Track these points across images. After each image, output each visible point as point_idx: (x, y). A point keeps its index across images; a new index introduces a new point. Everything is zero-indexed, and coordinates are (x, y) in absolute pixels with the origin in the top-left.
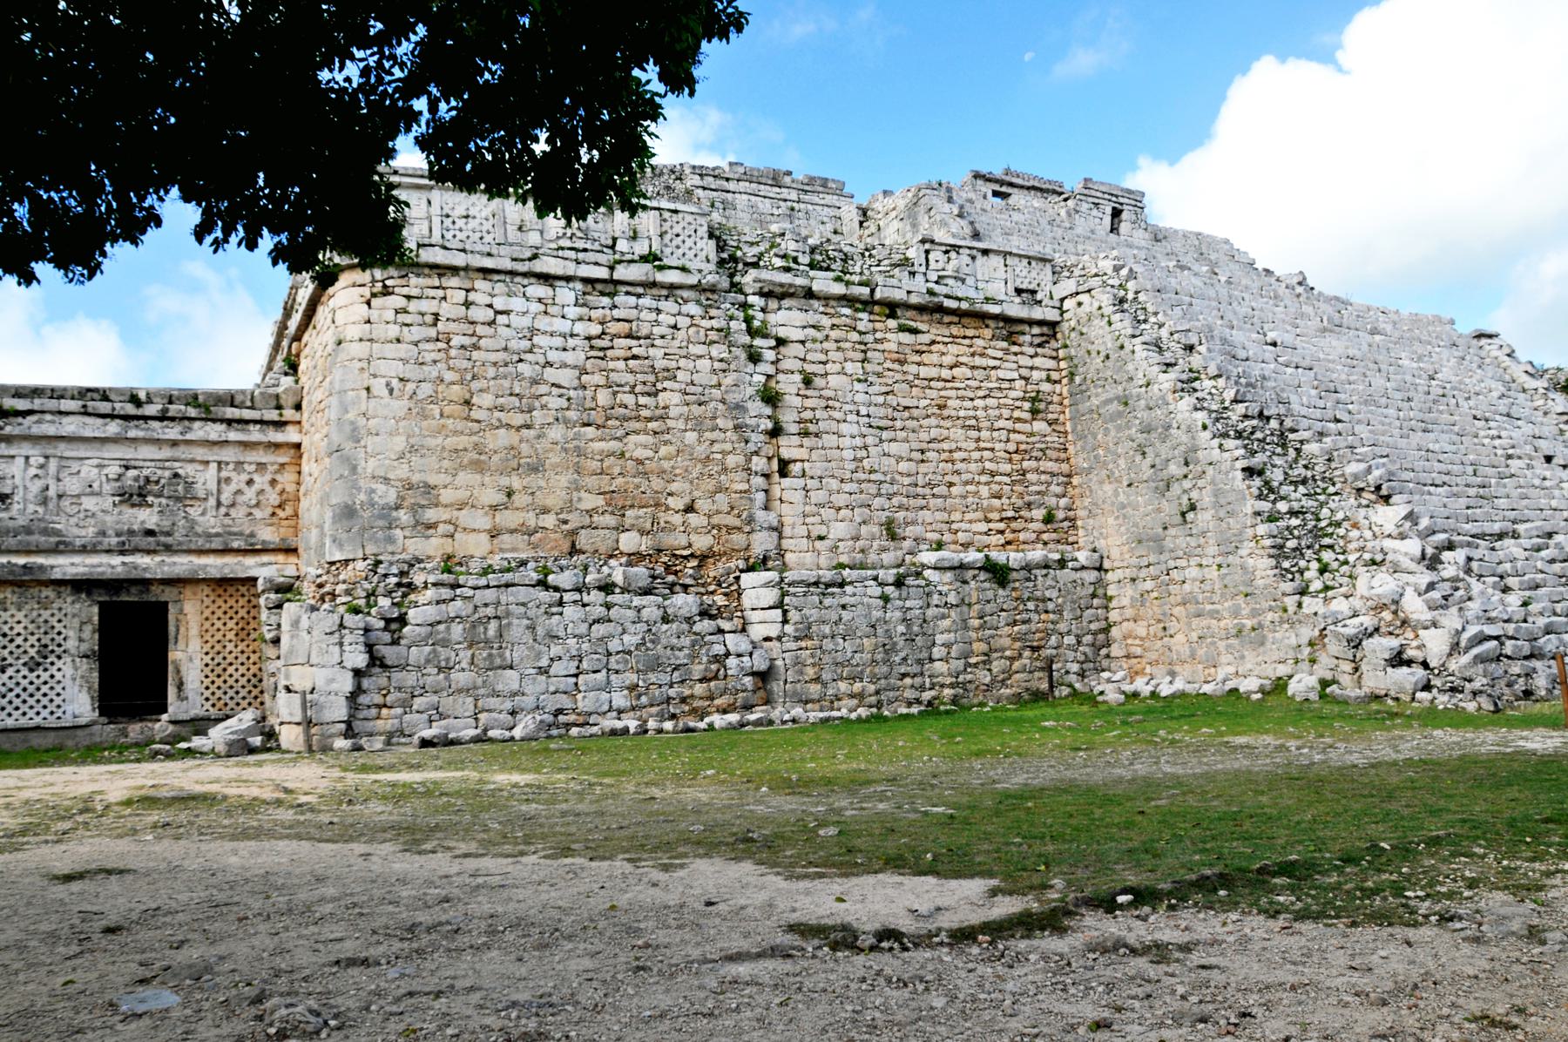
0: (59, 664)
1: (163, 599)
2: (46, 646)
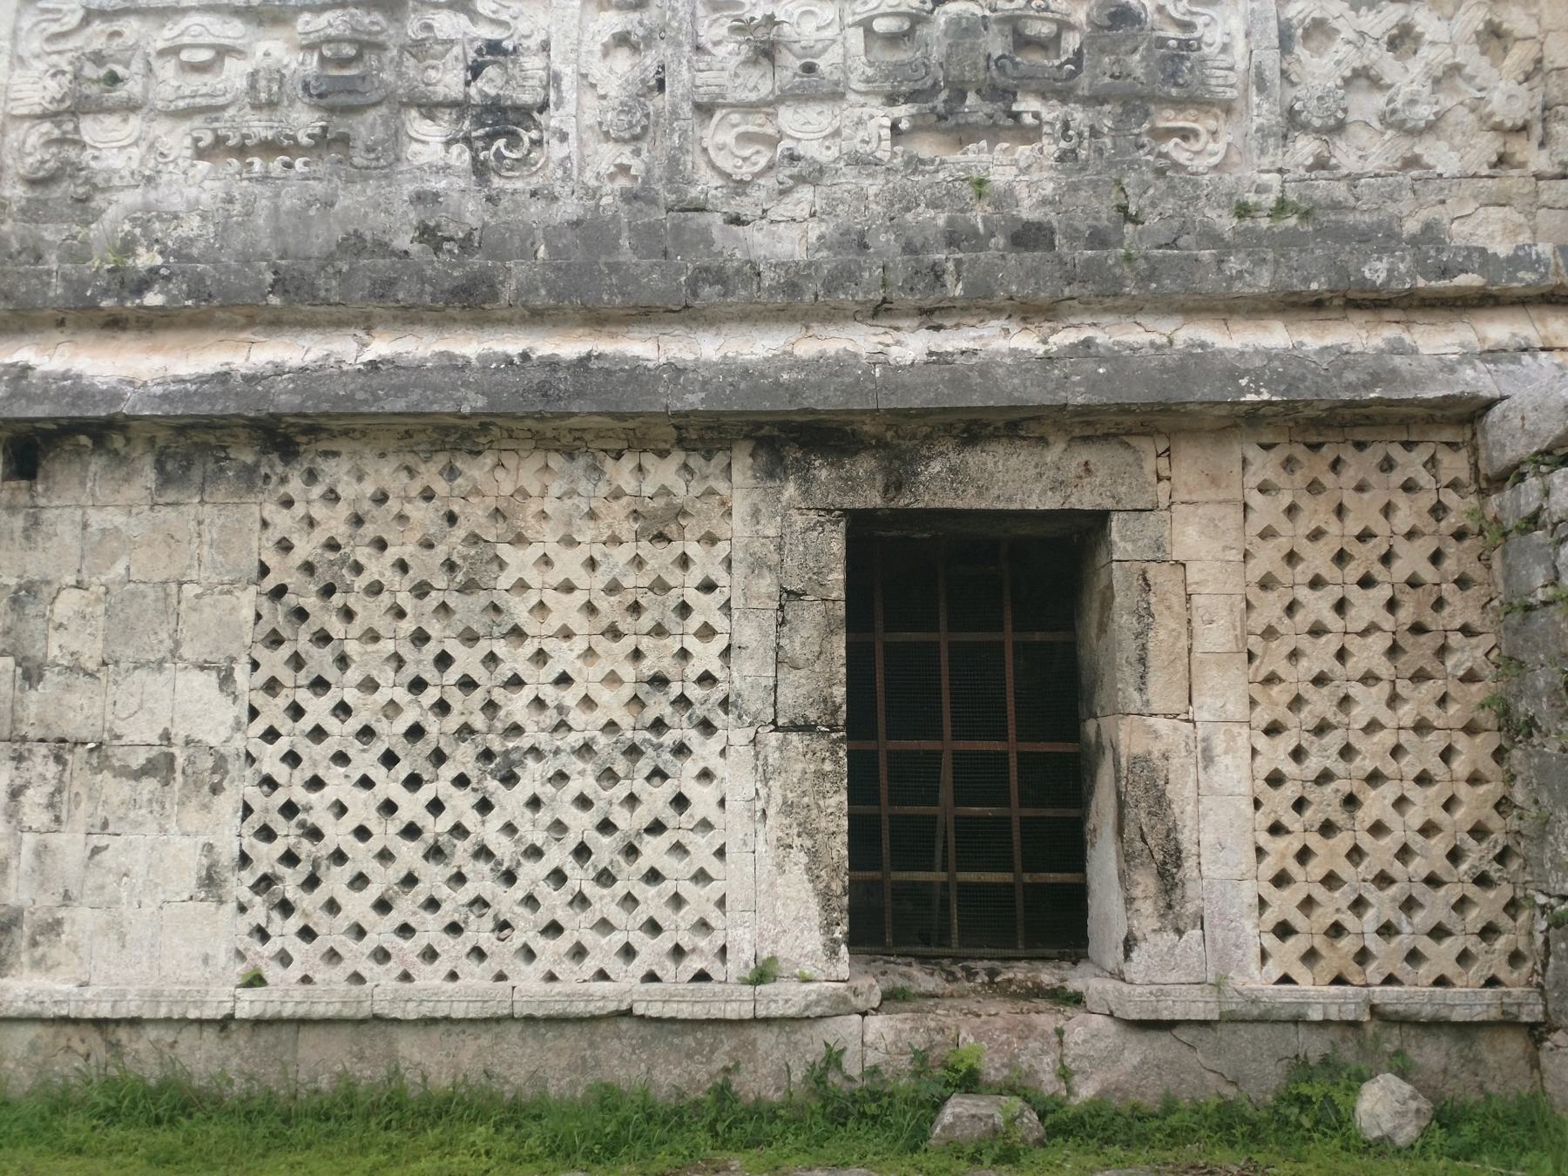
0: (705, 751)
1: (1085, 499)
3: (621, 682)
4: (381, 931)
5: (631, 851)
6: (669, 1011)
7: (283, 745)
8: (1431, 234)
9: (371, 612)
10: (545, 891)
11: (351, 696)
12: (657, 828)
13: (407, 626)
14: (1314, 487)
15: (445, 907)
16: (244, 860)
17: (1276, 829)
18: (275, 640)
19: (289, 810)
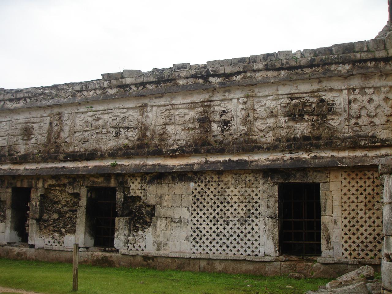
0: (256, 221)
2: (249, 210)
3: (243, 210)
4: (210, 246)
5: (246, 236)
6: (251, 259)
7: (196, 219)
8: (374, 136)
9: (208, 199)
10: (233, 241)
11: (206, 212)
12: (249, 233)
13: (213, 201)
14: (353, 179)
15: (219, 243)
16: (192, 235)
17: (346, 234)
18: (195, 203)
19: (197, 228)
